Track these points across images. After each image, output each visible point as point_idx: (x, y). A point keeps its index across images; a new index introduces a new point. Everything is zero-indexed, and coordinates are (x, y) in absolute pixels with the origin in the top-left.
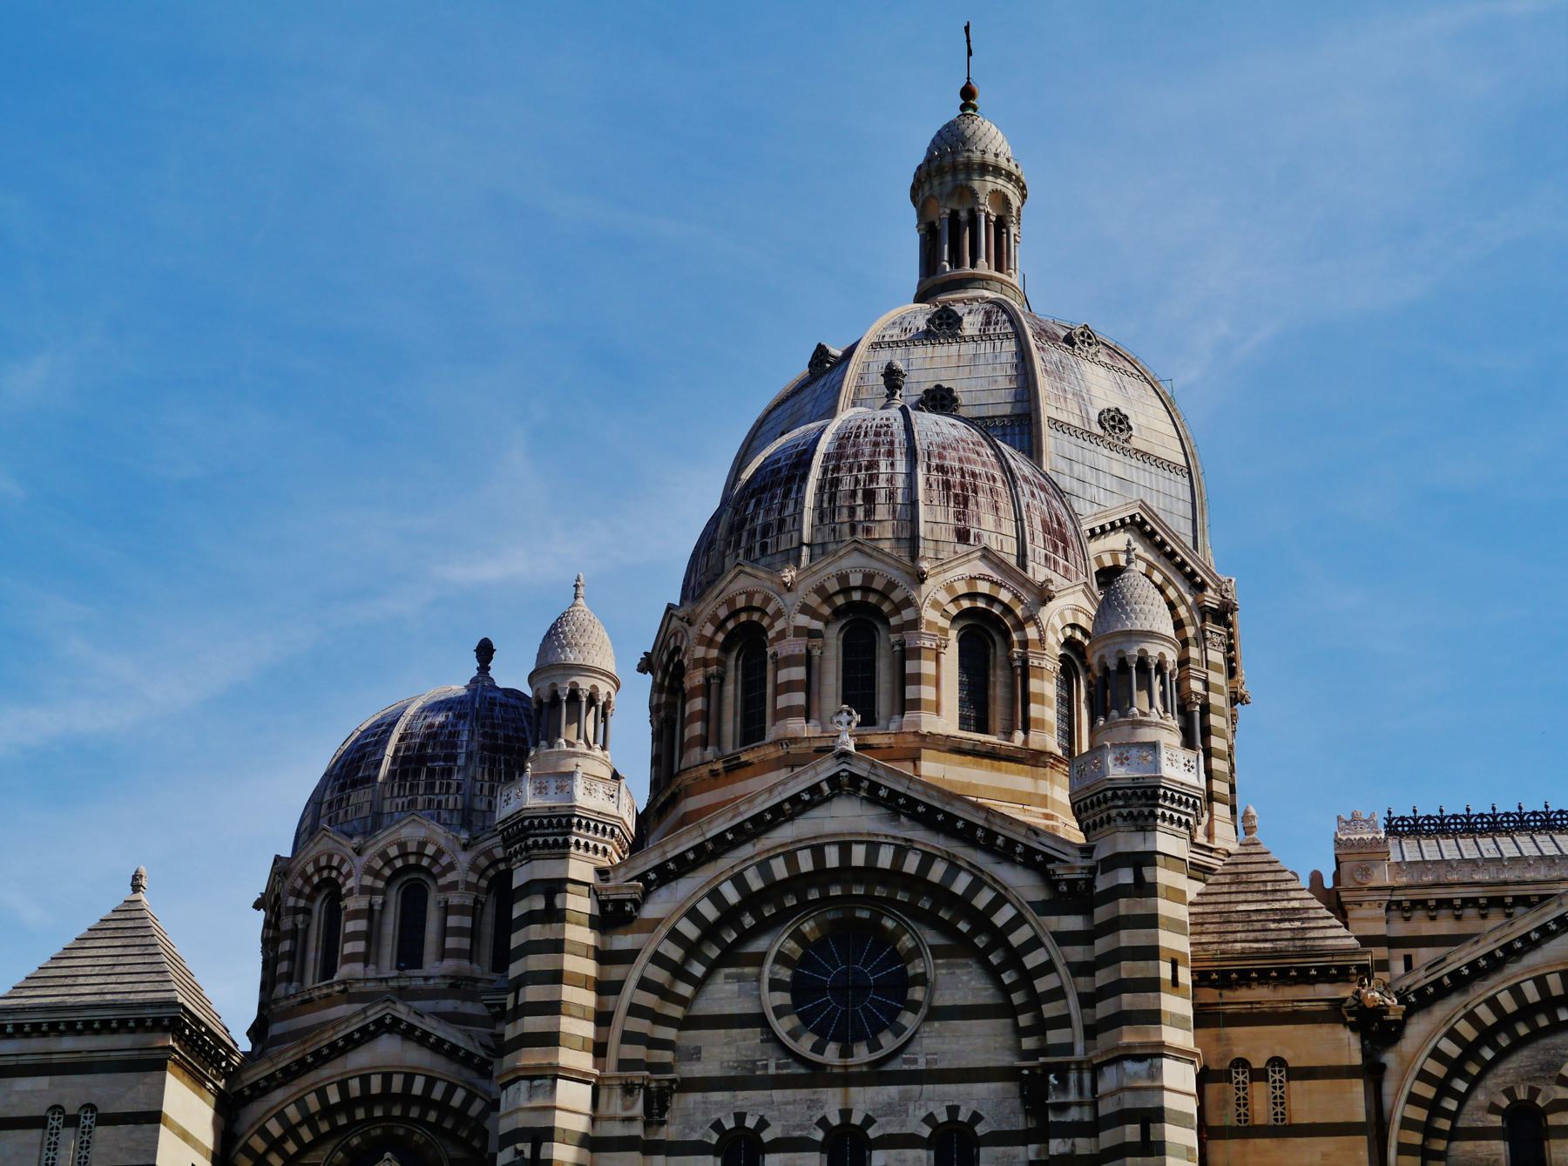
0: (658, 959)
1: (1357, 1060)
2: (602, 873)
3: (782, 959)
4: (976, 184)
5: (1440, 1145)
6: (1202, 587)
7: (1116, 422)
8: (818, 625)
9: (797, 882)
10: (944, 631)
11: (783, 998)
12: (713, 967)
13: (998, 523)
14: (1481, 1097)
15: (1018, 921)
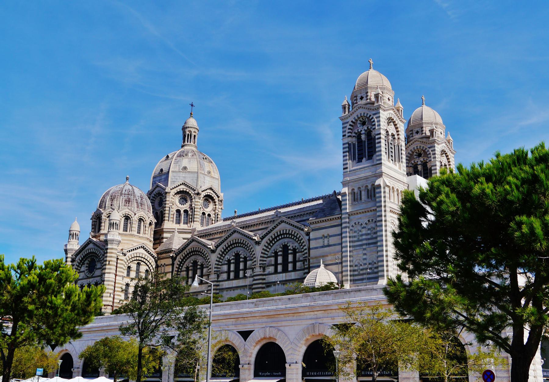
0: (77, 265)
1: (171, 263)
2: (72, 255)
3: (87, 264)
4: (186, 130)
5: (179, 273)
6: (195, 190)
7: (185, 168)
8: (95, 220)
9: (87, 254)
10: (106, 219)
11: (87, 268)
12: (82, 265)
13: (117, 202)
14: (184, 266)
15: (101, 257)
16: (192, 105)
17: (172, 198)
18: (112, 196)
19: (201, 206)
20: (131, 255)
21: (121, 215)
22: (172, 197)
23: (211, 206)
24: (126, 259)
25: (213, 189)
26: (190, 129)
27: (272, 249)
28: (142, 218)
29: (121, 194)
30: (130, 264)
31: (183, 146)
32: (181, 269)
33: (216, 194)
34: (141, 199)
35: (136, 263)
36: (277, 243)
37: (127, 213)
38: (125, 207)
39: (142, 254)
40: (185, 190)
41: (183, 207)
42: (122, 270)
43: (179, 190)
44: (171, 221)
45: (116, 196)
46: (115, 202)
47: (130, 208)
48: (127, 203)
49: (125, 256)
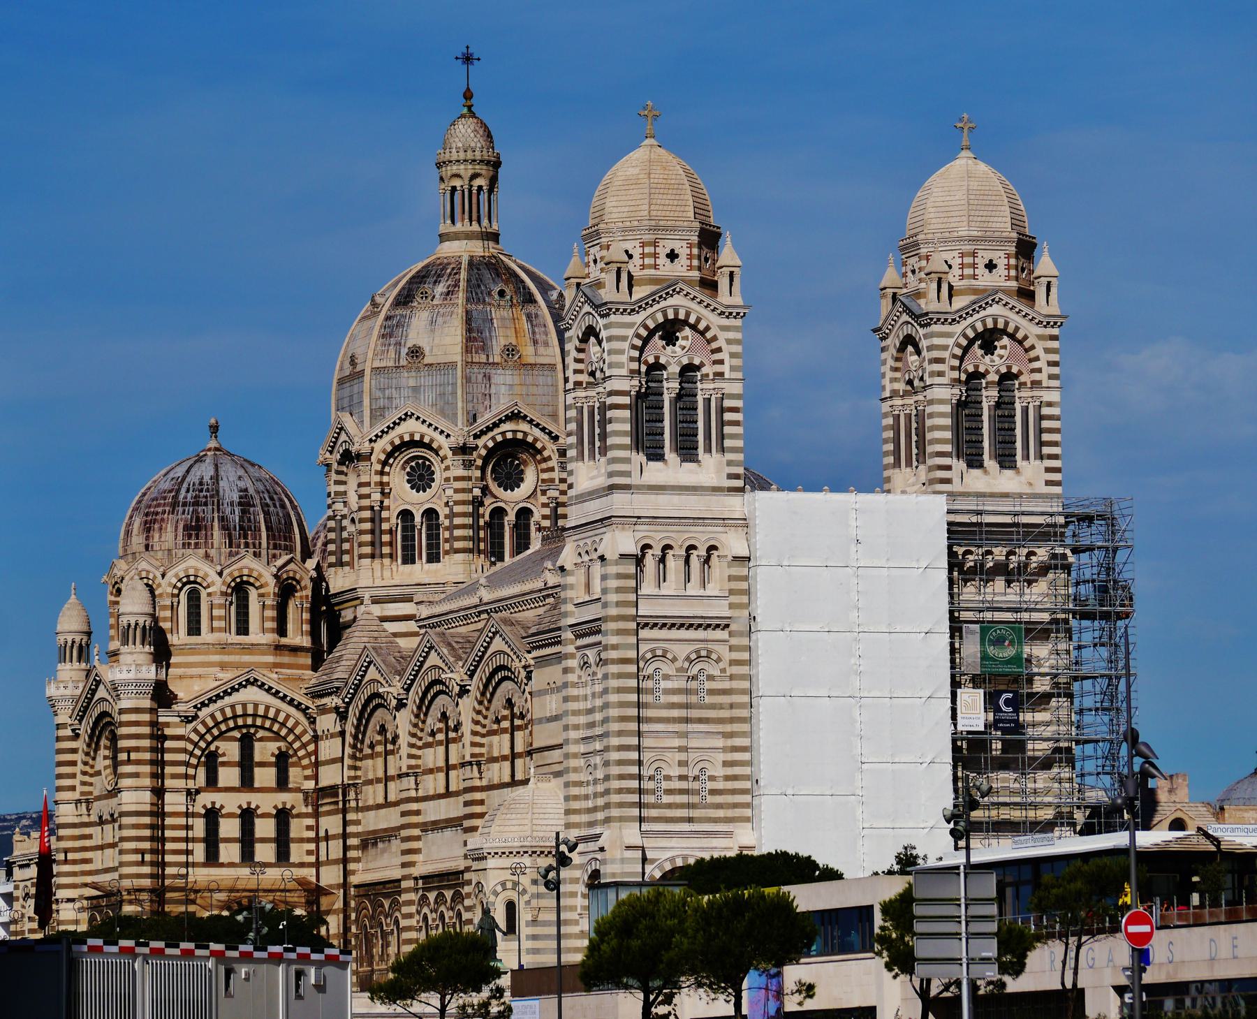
3: (106, 747)
5: (359, 764)
7: (416, 352)
12: (96, 751)
16: (468, 59)
17: (377, 473)
18: (147, 515)
19: (477, 492)
20: (212, 716)
21: (174, 581)
22: (379, 467)
23: (530, 476)
24: (195, 730)
25: (526, 416)
26: (454, 169)
27: (492, 709)
28: (245, 578)
29: (174, 504)
30: (216, 743)
31: (443, 237)
32: (361, 751)
33: (543, 429)
34: (244, 512)
35: (234, 739)
36: (499, 691)
37: (191, 572)
38: (189, 551)
39: (256, 706)
40: (417, 438)
41: (417, 502)
42: (182, 770)
43: (397, 442)
44: (382, 556)
45: (157, 513)
46: (157, 535)
47: (201, 552)
48: (191, 535)
49: (191, 722)
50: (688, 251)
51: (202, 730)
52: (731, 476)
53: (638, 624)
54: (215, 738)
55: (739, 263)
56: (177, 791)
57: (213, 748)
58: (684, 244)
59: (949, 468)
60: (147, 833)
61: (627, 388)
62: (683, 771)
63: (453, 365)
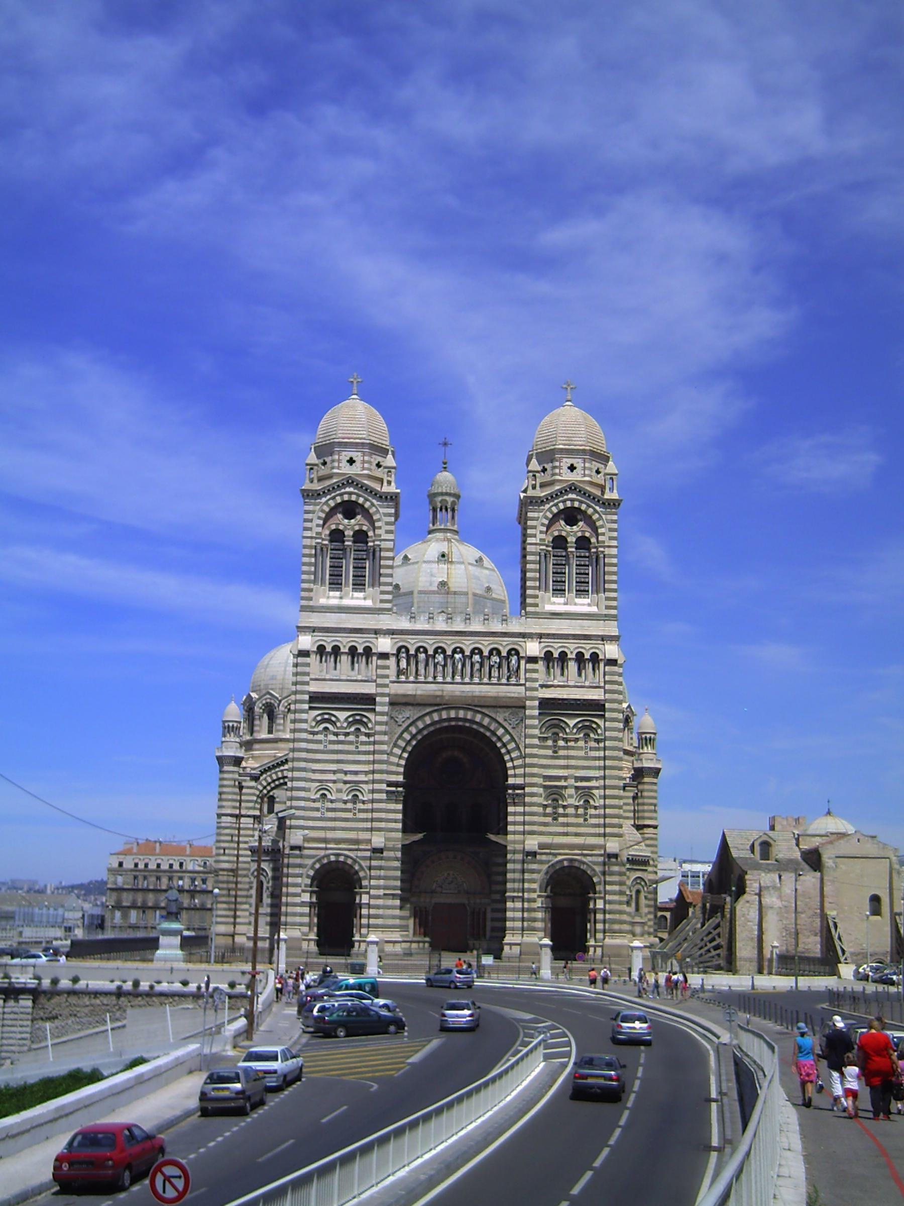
16: (445, 444)
21: (260, 705)
24: (261, 784)
30: (274, 791)
37: (268, 700)
50: (362, 459)
51: (265, 783)
52: (382, 601)
53: (310, 697)
54: (273, 789)
55: (394, 465)
56: (249, 816)
57: (271, 794)
58: (359, 454)
59: (536, 597)
60: (229, 838)
61: (314, 544)
62: (340, 796)
63: (411, 593)
